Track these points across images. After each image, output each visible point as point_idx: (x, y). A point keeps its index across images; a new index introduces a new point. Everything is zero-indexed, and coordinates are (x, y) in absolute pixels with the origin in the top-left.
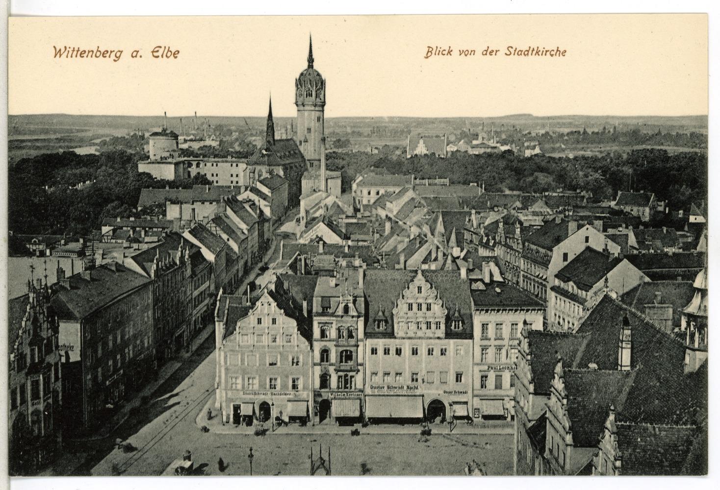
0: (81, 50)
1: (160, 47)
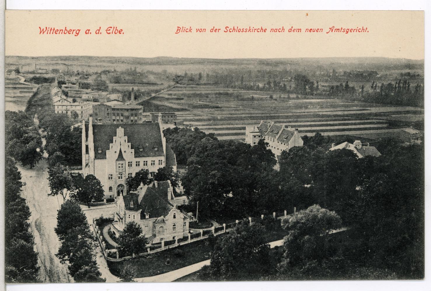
0: (55, 29)
1: (111, 27)
